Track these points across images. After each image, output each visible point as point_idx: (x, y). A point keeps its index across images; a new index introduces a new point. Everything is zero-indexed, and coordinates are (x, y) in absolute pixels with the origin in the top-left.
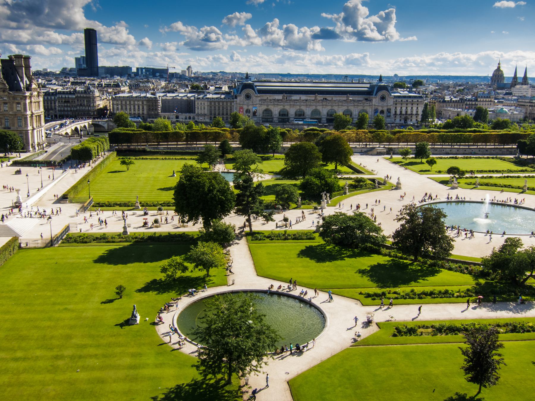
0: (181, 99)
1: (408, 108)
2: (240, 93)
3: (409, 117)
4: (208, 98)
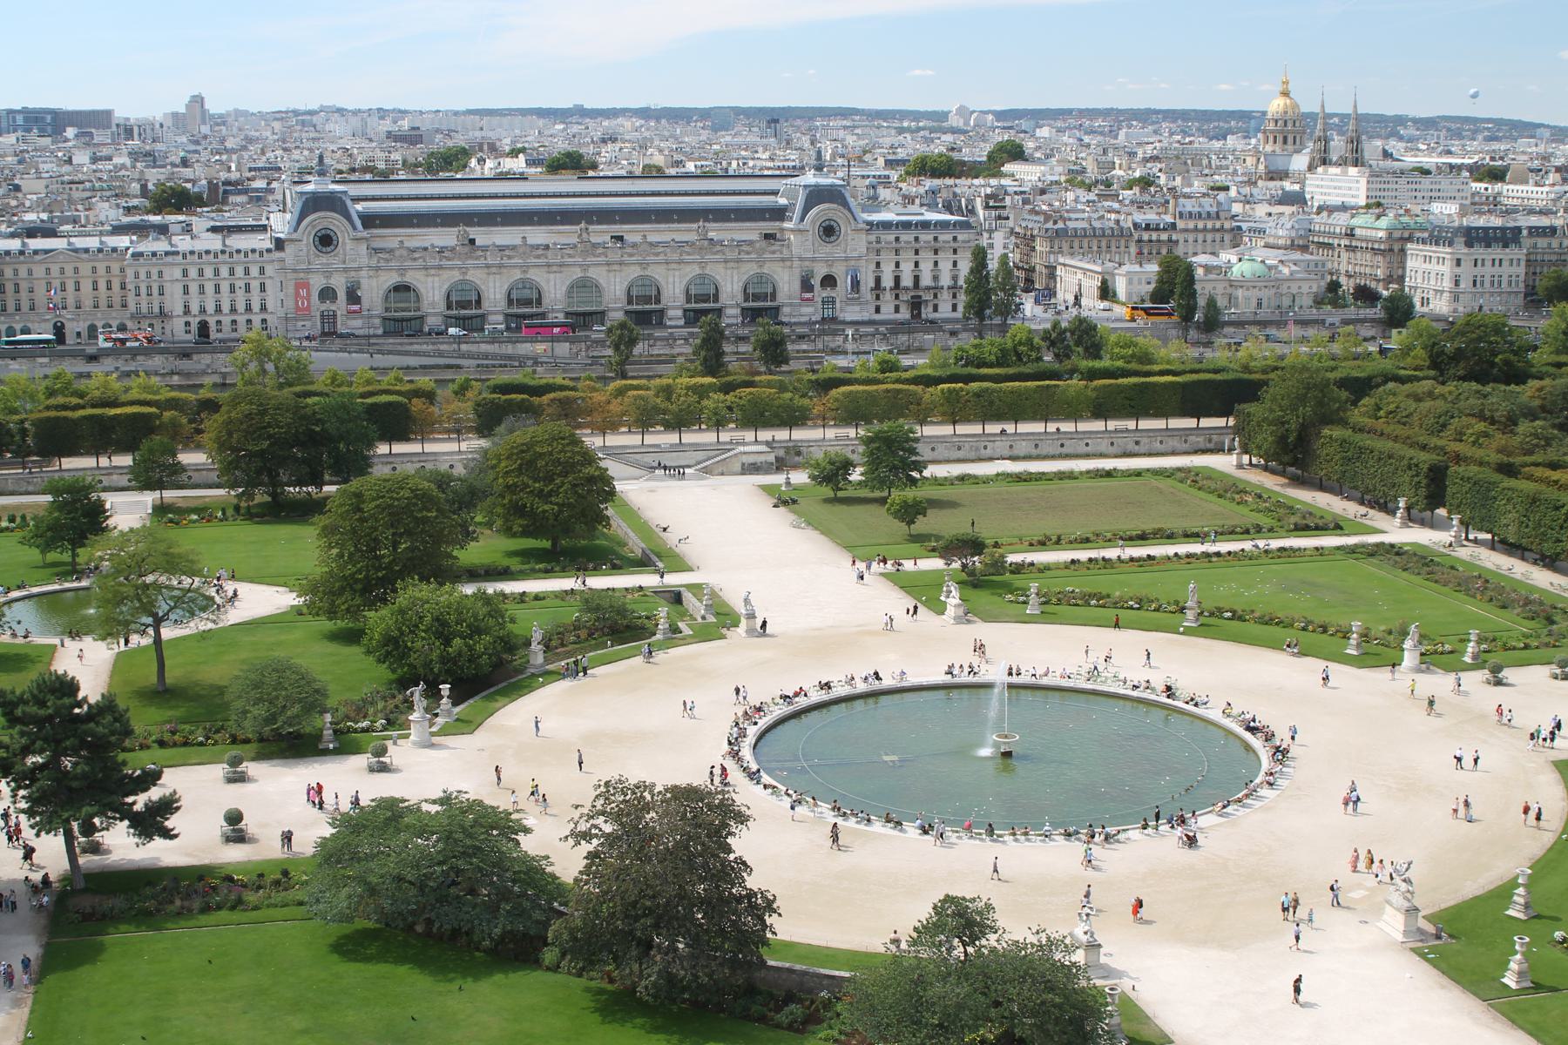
1: (922, 266)
3: (928, 296)
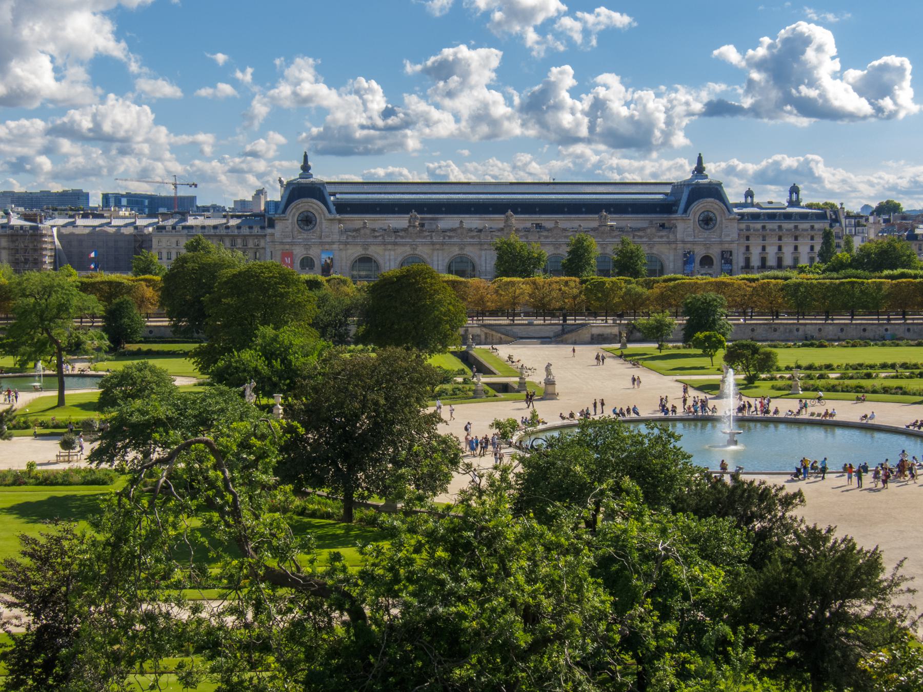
0: (118, 235)
1: (784, 249)
2: (284, 212)
4: (191, 227)
